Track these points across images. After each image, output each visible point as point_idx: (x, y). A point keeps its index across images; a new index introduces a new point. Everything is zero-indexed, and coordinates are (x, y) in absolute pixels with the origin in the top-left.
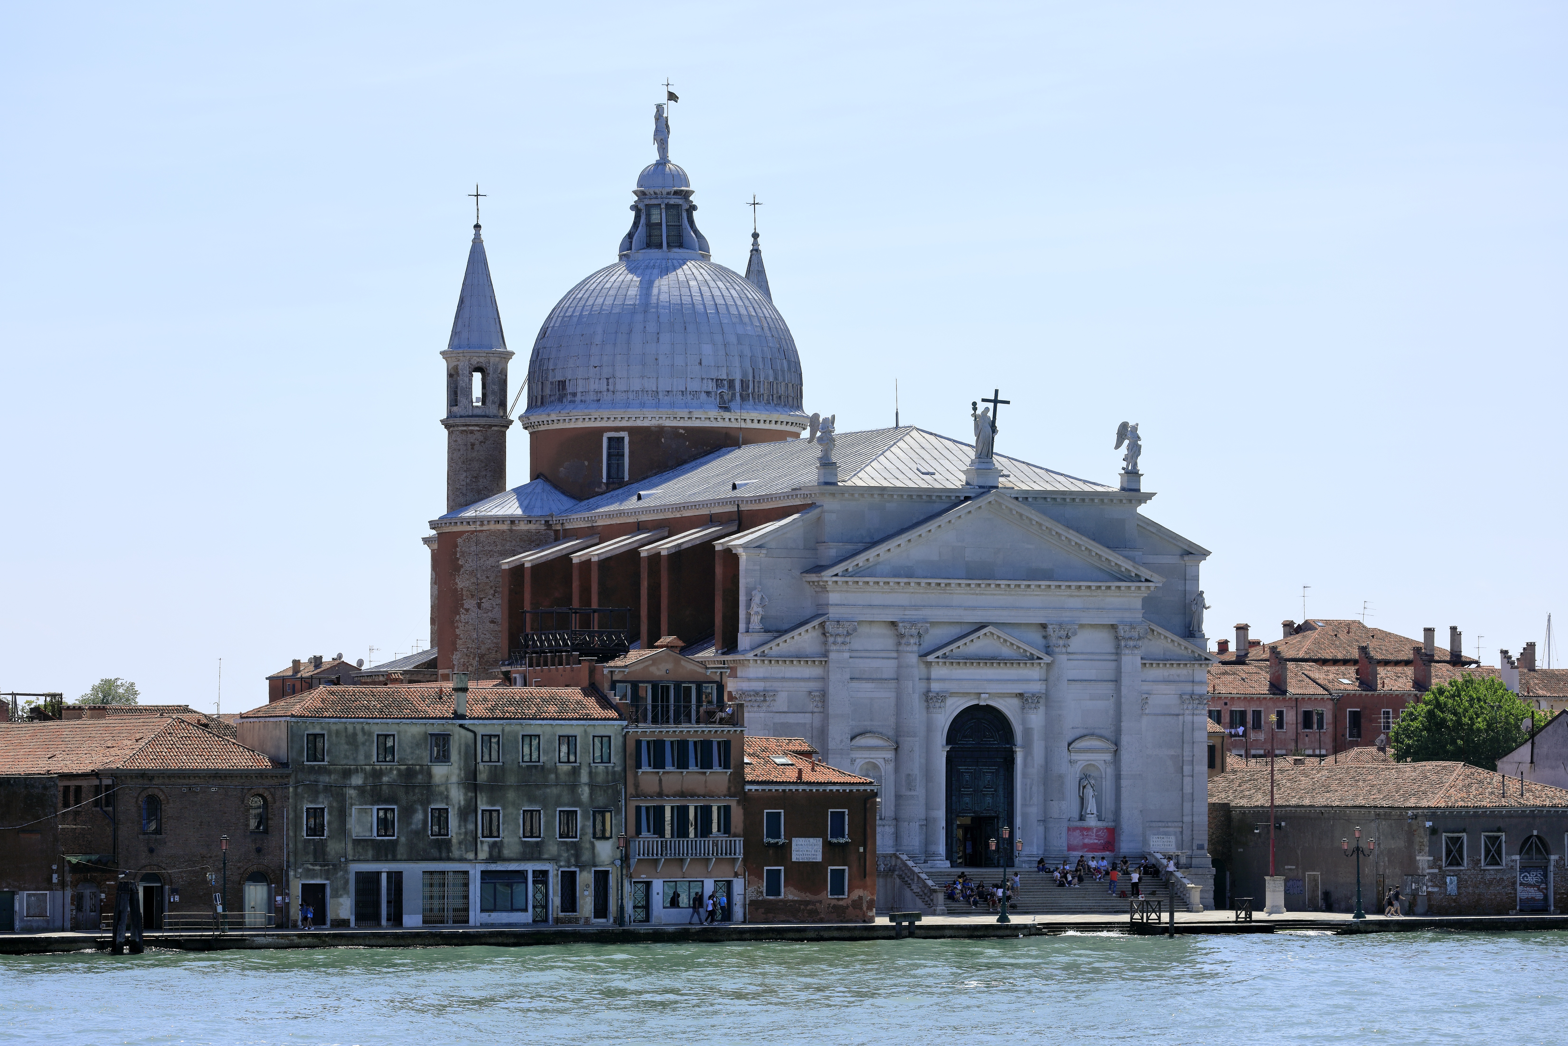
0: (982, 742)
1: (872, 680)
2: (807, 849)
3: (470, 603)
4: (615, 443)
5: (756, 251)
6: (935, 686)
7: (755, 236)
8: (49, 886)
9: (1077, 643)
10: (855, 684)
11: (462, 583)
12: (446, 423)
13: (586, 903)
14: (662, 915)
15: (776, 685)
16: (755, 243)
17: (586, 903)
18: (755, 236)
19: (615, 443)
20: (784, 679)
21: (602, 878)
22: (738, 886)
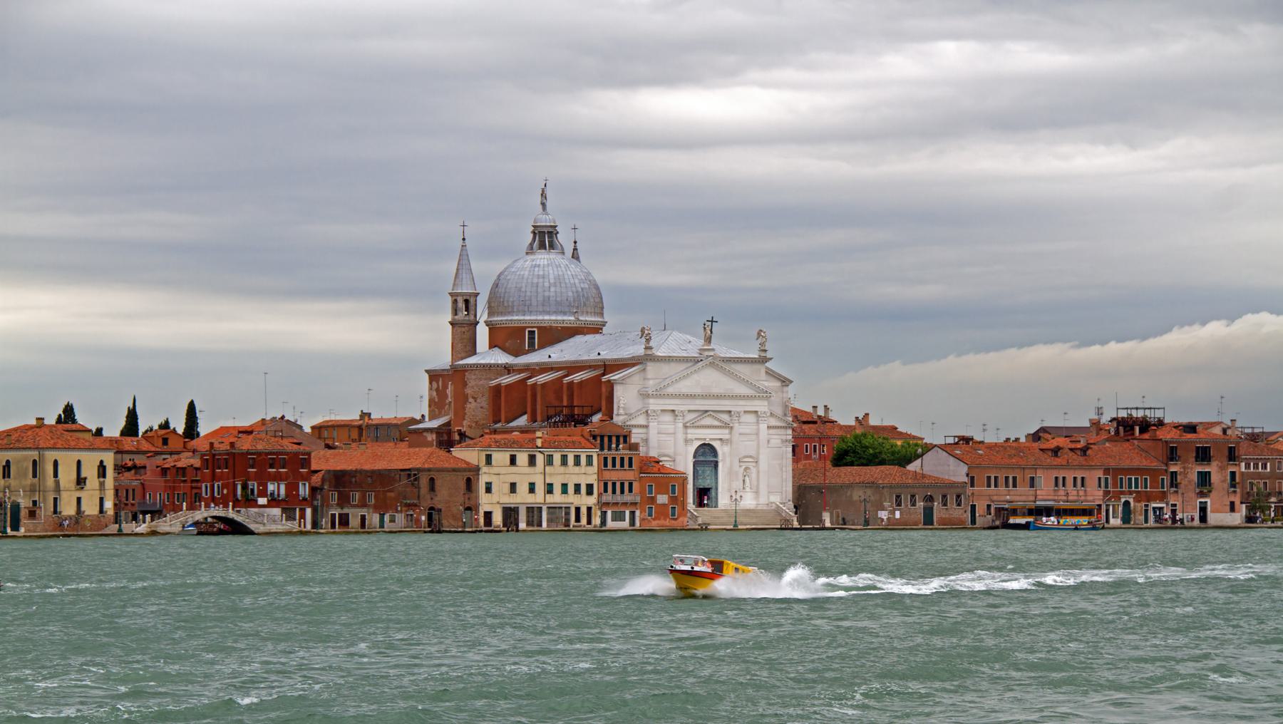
0: (707, 455)
2: (662, 499)
3: (471, 400)
4: (532, 333)
5: (575, 249)
6: (689, 436)
8: (397, 511)
11: (469, 391)
12: (452, 323)
13: (584, 520)
14: (611, 524)
17: (584, 520)
19: (532, 333)
21: (589, 509)
22: (638, 513)
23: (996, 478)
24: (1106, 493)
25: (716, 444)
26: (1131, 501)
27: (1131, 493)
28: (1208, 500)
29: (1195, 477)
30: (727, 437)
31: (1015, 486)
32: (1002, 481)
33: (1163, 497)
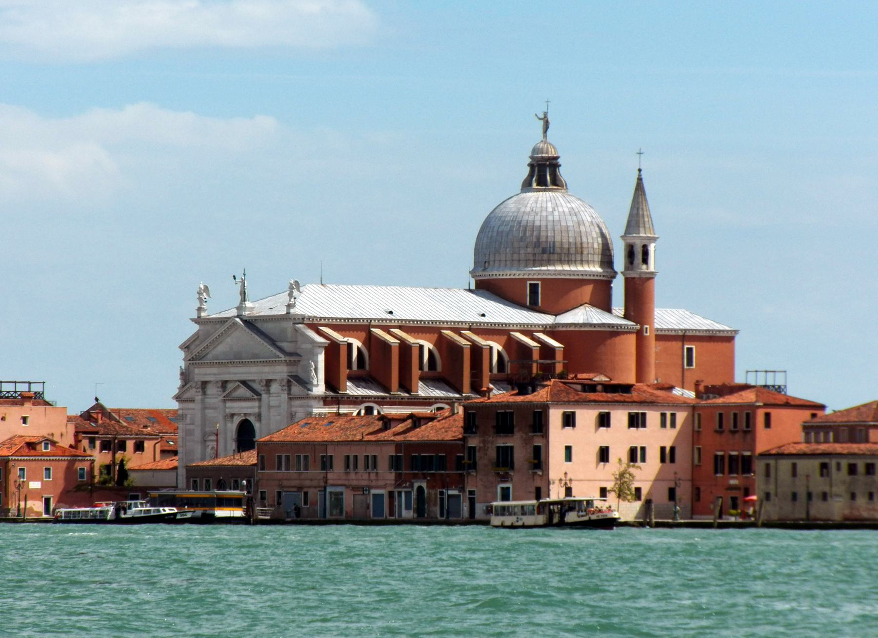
1: (212, 408)
5: (640, 180)
6: (227, 411)
7: (640, 170)
9: (275, 388)
10: (207, 411)
15: (186, 412)
16: (640, 175)
18: (640, 170)
20: (188, 409)
23: (287, 457)
24: (398, 477)
25: (252, 419)
26: (424, 485)
27: (424, 477)
28: (509, 485)
29: (492, 454)
30: (256, 410)
31: (306, 469)
32: (293, 461)
33: (460, 482)
